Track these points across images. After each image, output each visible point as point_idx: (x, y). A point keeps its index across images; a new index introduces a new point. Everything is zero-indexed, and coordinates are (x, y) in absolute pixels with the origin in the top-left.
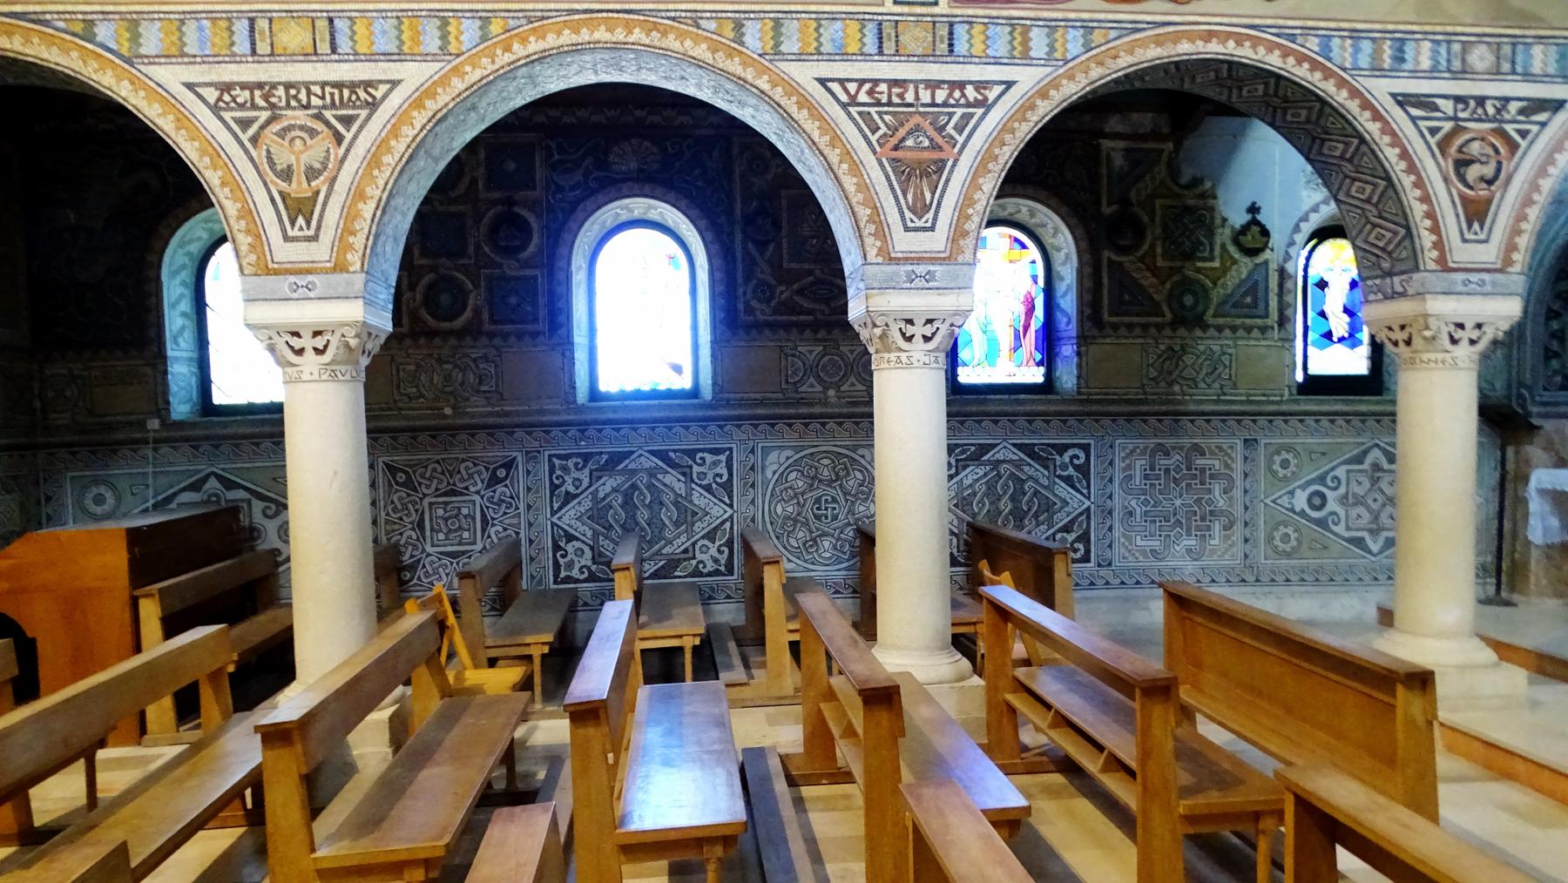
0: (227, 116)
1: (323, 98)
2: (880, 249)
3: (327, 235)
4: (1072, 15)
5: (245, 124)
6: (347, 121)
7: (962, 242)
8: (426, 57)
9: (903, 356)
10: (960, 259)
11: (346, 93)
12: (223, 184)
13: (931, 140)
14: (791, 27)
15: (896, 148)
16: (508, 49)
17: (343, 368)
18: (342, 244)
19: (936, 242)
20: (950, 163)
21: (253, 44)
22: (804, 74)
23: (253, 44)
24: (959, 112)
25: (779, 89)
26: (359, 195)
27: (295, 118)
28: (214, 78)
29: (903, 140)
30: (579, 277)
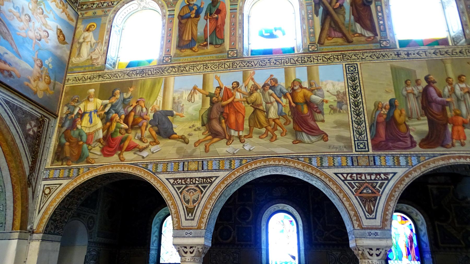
0: (175, 186)
1: (199, 181)
2: (358, 225)
3: (197, 219)
4: (412, 153)
5: (179, 188)
6: (204, 187)
7: (386, 223)
8: (225, 170)
9: (370, 261)
10: (386, 228)
11: (205, 180)
12: (172, 204)
13: (372, 190)
14: (325, 159)
15: (361, 193)
16: (247, 167)
17: (197, 258)
18: (200, 222)
19: (377, 222)
20: (379, 197)
21: (183, 168)
22: (330, 172)
23: (183, 168)
24: (380, 182)
25: (323, 176)
26: (205, 207)
27: (192, 187)
28: (173, 177)
29: (363, 190)
30: (263, 227)
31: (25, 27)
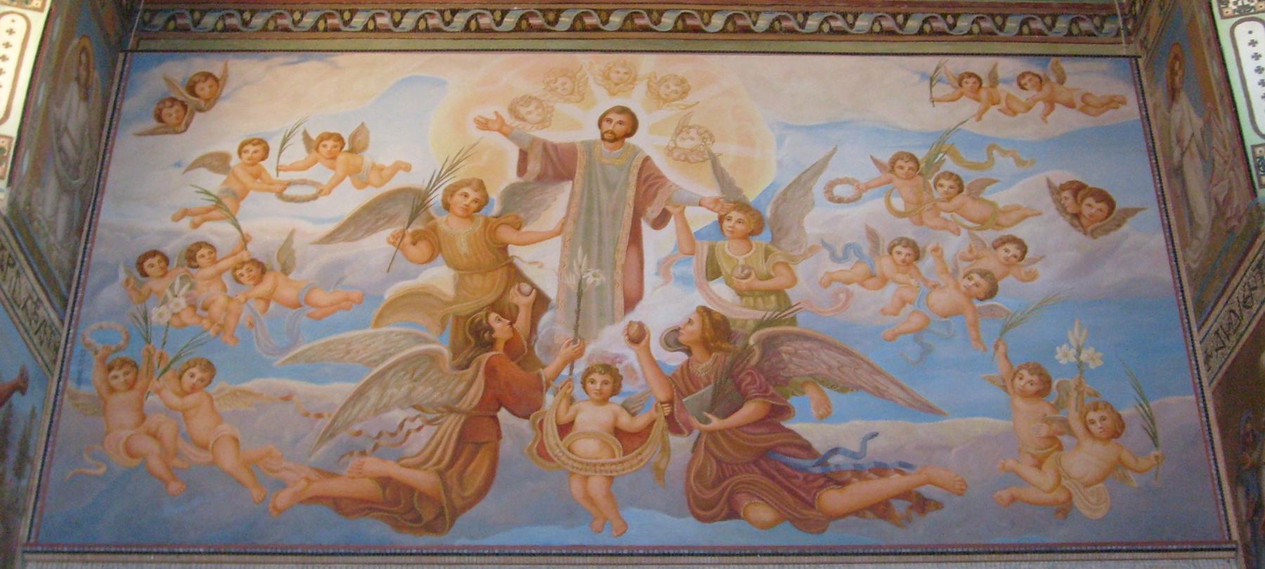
31: (906, 293)
